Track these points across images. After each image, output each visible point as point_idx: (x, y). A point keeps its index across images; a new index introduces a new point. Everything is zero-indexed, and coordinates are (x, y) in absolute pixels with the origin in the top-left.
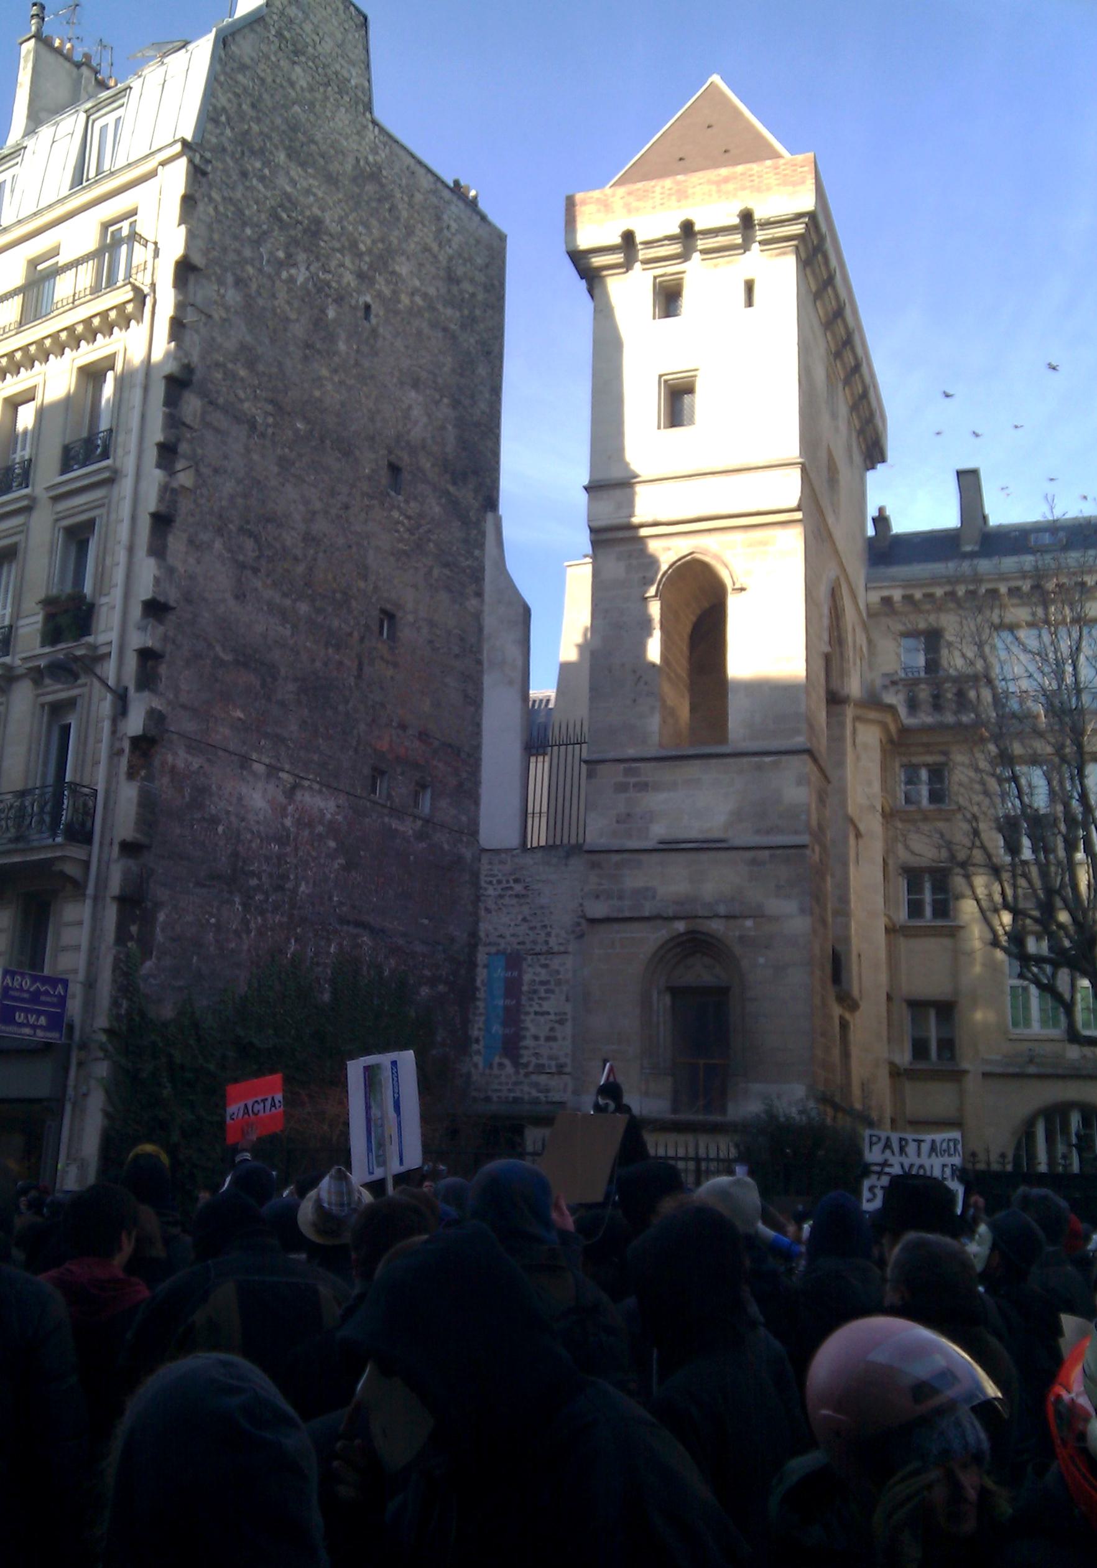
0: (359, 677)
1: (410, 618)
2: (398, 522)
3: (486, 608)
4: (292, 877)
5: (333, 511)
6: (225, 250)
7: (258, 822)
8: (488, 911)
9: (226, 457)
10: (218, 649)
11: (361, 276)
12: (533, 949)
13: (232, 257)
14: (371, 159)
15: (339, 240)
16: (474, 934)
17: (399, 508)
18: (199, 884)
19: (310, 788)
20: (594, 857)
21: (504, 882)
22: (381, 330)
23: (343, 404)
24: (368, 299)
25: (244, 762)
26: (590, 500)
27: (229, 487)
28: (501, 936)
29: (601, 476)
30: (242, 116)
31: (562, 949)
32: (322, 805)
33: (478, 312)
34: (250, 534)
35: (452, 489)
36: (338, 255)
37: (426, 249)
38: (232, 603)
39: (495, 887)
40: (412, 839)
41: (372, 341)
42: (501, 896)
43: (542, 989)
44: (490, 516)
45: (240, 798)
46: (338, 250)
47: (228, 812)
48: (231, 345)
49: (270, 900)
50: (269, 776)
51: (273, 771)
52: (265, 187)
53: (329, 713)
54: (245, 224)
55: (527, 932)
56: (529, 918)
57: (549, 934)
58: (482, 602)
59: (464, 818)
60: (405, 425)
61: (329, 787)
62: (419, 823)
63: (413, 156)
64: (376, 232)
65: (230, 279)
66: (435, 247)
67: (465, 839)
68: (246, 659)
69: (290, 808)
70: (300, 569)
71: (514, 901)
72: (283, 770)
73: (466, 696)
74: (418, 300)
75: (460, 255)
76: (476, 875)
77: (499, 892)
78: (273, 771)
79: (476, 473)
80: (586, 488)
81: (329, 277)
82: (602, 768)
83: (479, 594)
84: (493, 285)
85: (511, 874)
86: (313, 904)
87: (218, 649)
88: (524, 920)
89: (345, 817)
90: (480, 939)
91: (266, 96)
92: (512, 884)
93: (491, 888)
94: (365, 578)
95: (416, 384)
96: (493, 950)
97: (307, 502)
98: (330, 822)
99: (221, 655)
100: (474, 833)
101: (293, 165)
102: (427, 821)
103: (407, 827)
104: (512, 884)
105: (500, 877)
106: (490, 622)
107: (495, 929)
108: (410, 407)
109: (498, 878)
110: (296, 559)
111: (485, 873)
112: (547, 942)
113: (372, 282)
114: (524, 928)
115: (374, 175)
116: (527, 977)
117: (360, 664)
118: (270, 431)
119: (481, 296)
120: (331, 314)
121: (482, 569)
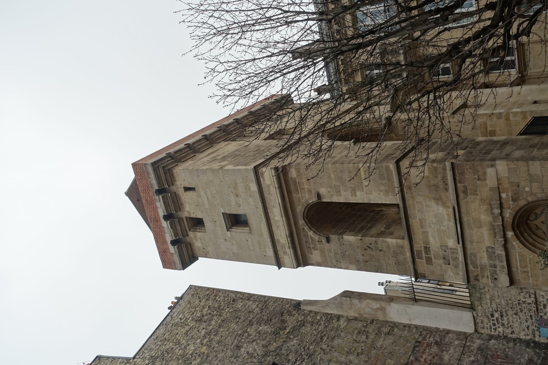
3: (345, 314)
8: (513, 332)
12: (535, 312)
16: (527, 343)
20: (472, 279)
21: (494, 322)
28: (528, 328)
29: (273, 260)
31: (533, 296)
33: (216, 306)
37: (186, 334)
39: (497, 327)
42: (503, 325)
55: (523, 313)
56: (515, 312)
58: (342, 316)
59: (456, 343)
60: (255, 357)
66: (187, 328)
67: (469, 344)
71: (505, 318)
73: (388, 334)
75: (193, 313)
76: (491, 337)
77: (500, 325)
79: (282, 314)
80: (279, 268)
82: (420, 270)
83: (339, 317)
84: (208, 295)
85: (489, 318)
88: (516, 314)
90: (531, 339)
92: (495, 318)
93: (498, 329)
95: (238, 347)
96: (537, 333)
100: (465, 336)
104: (495, 318)
105: (491, 324)
106: (352, 314)
107: (524, 330)
108: (248, 353)
109: (492, 325)
111: (489, 332)
112: (529, 304)
114: (520, 314)
119: (210, 303)
121: (326, 314)
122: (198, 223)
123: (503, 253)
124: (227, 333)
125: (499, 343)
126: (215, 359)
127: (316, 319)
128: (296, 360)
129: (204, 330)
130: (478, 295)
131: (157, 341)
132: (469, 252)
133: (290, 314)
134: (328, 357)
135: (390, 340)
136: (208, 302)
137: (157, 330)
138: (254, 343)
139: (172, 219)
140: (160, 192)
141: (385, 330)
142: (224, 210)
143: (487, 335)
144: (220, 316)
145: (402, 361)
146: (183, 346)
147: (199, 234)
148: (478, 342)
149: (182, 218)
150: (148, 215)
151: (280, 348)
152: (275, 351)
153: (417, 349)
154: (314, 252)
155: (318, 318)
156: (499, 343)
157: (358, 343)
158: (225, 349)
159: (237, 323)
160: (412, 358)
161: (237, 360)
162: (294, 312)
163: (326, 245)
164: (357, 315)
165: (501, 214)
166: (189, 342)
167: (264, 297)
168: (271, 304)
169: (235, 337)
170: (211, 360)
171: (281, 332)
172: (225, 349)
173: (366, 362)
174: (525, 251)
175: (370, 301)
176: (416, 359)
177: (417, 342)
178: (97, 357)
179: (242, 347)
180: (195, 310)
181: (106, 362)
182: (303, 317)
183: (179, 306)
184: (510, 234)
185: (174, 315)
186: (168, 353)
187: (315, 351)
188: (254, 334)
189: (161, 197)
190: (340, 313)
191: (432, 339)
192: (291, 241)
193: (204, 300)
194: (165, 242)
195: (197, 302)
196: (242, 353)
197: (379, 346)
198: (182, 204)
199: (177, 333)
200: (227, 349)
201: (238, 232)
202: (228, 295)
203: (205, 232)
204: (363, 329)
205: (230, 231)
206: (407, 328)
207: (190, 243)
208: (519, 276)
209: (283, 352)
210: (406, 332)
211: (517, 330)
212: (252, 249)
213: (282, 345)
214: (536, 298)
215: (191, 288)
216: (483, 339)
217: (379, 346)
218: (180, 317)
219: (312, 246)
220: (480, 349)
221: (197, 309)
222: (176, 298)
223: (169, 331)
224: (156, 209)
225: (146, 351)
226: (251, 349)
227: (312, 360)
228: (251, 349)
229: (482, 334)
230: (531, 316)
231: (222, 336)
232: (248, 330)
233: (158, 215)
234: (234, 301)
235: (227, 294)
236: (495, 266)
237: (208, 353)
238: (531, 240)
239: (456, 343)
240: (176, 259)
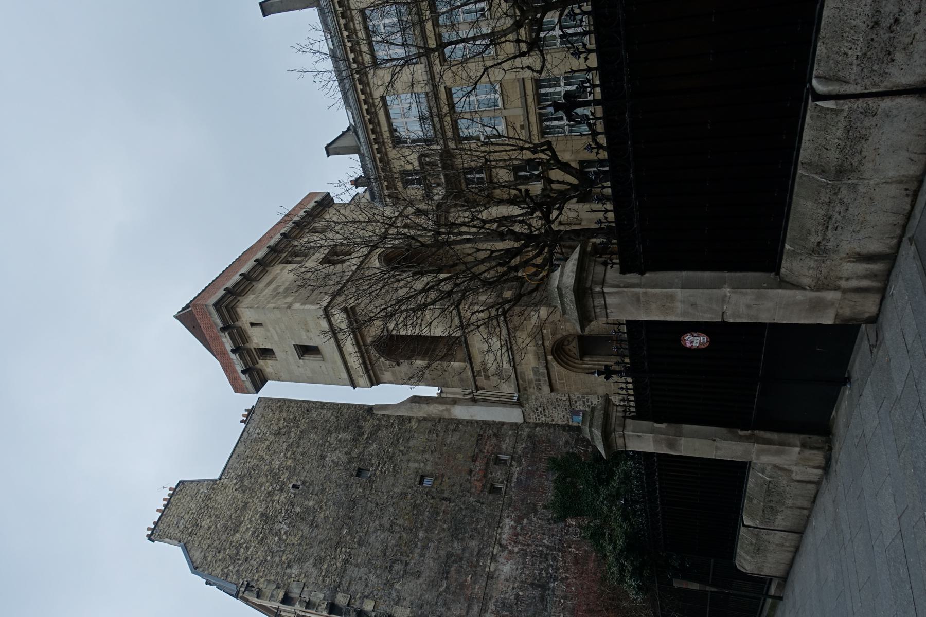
0: (449, 500)
1: (422, 465)
2: (381, 471)
3: (415, 415)
4: (541, 548)
5: (379, 513)
6: (277, 573)
7: (517, 569)
8: (552, 420)
9: (360, 579)
10: (441, 589)
11: (281, 490)
13: (279, 570)
14: (235, 481)
15: (269, 503)
17: (375, 470)
18: (545, 609)
19: (500, 534)
20: (521, 390)
22: (302, 478)
23: (334, 504)
24: (291, 486)
25: (490, 576)
26: (359, 386)
27: (372, 578)
28: (564, 417)
29: (348, 382)
30: (224, 560)
32: (507, 527)
33: (291, 417)
34: (391, 566)
35: (366, 436)
36: (274, 504)
37: (268, 448)
38: (421, 580)
40: (521, 468)
41: (307, 484)
42: (545, 416)
43: (586, 403)
44: (375, 412)
45: (506, 580)
46: (273, 503)
47: (513, 588)
48: (315, 572)
49: (552, 563)
50: (496, 561)
51: (494, 558)
52: (251, 546)
53: (466, 520)
54: (266, 560)
57: (561, 400)
58: (413, 417)
59: (510, 433)
61: (499, 523)
62: (514, 463)
63: (232, 455)
64: (264, 480)
65: (288, 571)
66: (267, 443)
67: (520, 433)
68: (445, 574)
69: (510, 548)
70: (405, 535)
71: (547, 411)
72: (493, 552)
73: (455, 430)
74: (288, 455)
75: (269, 427)
76: (536, 425)
78: (494, 558)
79: (358, 420)
81: (283, 511)
82: (480, 384)
83: (410, 419)
84: (280, 406)
86: (553, 535)
87: (441, 589)
88: (555, 408)
89: (513, 512)
91: (215, 545)
94: (406, 494)
95: (323, 457)
96: (570, 420)
97: (376, 530)
98: (515, 522)
99: (444, 587)
100: (515, 426)
101: (241, 529)
102: (512, 458)
103: (516, 470)
106: (421, 414)
108: (333, 461)
110: (400, 538)
113: (284, 483)
114: (558, 408)
115: (241, 478)
116: (582, 408)
117: (445, 499)
118: (348, 550)
119: (284, 414)
120: (298, 509)
121: (399, 417)
122: (266, 353)
123: (546, 371)
124: (309, 444)
125: (543, 430)
126: (303, 471)
127: (390, 422)
128: (379, 463)
129: (285, 444)
130: (525, 396)
131: (238, 460)
132: (518, 371)
133: (365, 421)
134: (407, 457)
135: (457, 436)
136: (282, 414)
137: (237, 448)
138: (337, 452)
139: (240, 351)
140: (223, 330)
141: (452, 427)
142: (295, 342)
143: (533, 423)
144: (298, 427)
145: (469, 454)
146: (268, 462)
147: (269, 362)
148: (527, 430)
149: (251, 349)
150: (214, 349)
151: (362, 453)
152: (358, 457)
153: (480, 442)
154: (385, 373)
155: (392, 421)
156: (543, 430)
157: (431, 441)
158: (310, 460)
159: (316, 433)
160: (477, 450)
161: (324, 470)
162: (368, 418)
163: (397, 368)
164: (425, 416)
165: (543, 344)
166: (273, 457)
167: (337, 404)
168: (345, 411)
169: (318, 447)
170: (299, 472)
171: (360, 439)
172: (310, 460)
173: (440, 458)
174: (562, 369)
175: (437, 405)
176: (481, 451)
177: (479, 435)
178: (180, 482)
179: (326, 456)
180: (271, 424)
181: (191, 485)
182: (377, 422)
183: (252, 421)
184: (550, 358)
185: (251, 431)
186: (254, 470)
187: (394, 453)
188: (335, 443)
189: (226, 333)
190: (411, 415)
191: (490, 431)
192: (364, 367)
193: (277, 412)
194: (235, 371)
195: (270, 415)
196: (328, 462)
197: (448, 443)
198: (249, 337)
199: (259, 449)
200: (312, 460)
201: (311, 362)
202: (301, 405)
203: (277, 360)
204: (433, 428)
205: (303, 359)
206: (470, 424)
207: (261, 370)
208: (557, 385)
209: (366, 457)
210: (469, 427)
211: (555, 419)
212: (327, 373)
213: (364, 451)
214: (569, 396)
215: (261, 401)
216: (530, 428)
217: (448, 443)
218: (256, 432)
219: (383, 369)
220: (529, 436)
221: (272, 422)
222: (246, 410)
223: (249, 448)
224: (223, 344)
225: (230, 471)
226: (335, 458)
227: (393, 462)
228: (335, 458)
229: (529, 423)
230: (566, 409)
231: (304, 448)
232: (329, 439)
233: (225, 349)
234: (308, 411)
235: (299, 404)
236: (539, 380)
237: (294, 466)
238: (565, 360)
239: (510, 433)
240: (249, 385)
